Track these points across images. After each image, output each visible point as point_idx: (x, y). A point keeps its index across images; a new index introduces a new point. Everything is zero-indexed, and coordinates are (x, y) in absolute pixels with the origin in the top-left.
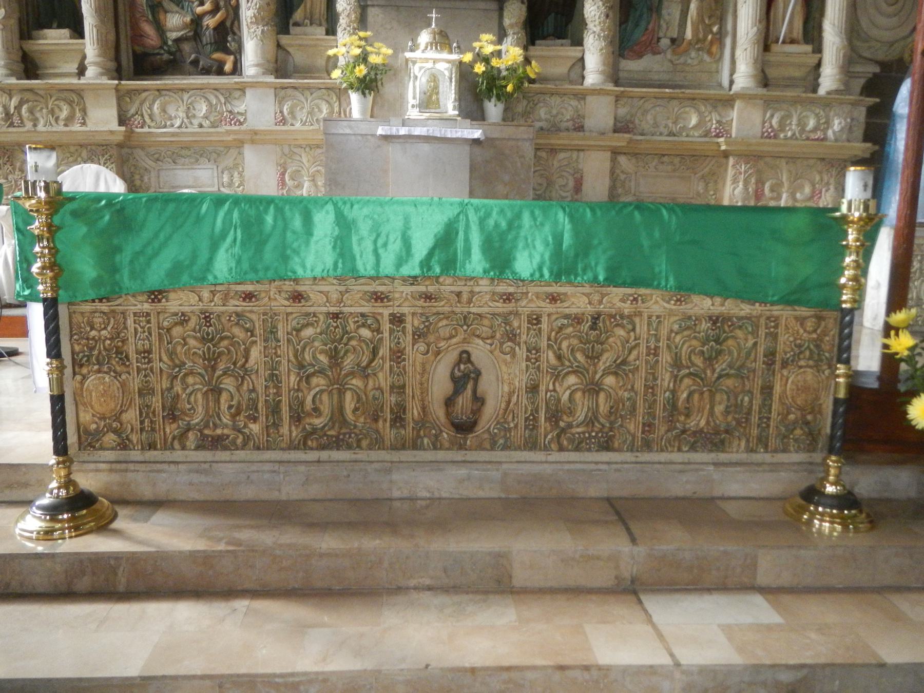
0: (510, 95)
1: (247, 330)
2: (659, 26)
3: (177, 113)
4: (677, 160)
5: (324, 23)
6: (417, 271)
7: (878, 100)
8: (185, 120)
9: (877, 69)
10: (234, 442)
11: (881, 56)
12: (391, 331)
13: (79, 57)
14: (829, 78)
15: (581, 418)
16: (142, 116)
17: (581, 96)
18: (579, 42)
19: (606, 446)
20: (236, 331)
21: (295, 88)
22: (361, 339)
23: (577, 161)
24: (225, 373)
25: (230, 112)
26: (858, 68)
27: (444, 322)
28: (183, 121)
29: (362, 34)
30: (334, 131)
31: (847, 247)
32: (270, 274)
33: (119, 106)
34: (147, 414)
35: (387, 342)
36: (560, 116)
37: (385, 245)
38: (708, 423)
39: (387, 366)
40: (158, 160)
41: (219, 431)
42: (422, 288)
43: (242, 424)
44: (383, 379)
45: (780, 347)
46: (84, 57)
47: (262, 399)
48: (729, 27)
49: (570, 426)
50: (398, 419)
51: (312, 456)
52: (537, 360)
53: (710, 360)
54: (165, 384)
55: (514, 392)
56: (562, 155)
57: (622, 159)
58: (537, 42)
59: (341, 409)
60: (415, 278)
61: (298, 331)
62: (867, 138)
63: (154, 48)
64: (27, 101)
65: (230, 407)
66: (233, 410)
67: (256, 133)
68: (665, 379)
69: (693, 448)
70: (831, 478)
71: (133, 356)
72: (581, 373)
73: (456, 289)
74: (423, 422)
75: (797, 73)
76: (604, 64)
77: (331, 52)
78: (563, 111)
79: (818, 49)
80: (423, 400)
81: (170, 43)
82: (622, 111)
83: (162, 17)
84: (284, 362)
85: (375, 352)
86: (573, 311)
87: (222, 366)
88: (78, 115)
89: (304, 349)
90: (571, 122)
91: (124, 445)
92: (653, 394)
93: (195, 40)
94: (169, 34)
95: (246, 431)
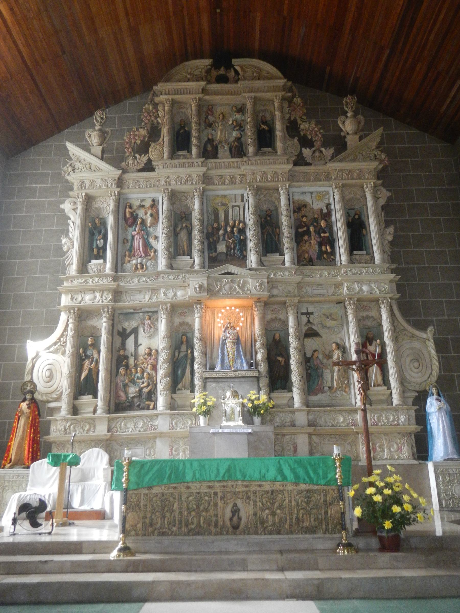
0: (263, 414)
1: (174, 498)
2: (323, 383)
3: (131, 426)
4: (337, 436)
5: (189, 388)
6: (221, 479)
7: (418, 407)
9: (417, 394)
10: (168, 533)
11: (417, 389)
12: (214, 497)
13: (94, 406)
16: (117, 428)
17: (293, 412)
18: (291, 391)
19: (279, 533)
20: (171, 499)
22: (205, 500)
23: (294, 439)
24: (167, 511)
25: (152, 425)
26: (409, 394)
27: (229, 494)
29: (204, 393)
30: (193, 432)
31: (337, 467)
32: (181, 481)
35: (213, 501)
36: (285, 421)
37: (212, 472)
38: (309, 524)
39: (213, 508)
41: (164, 530)
42: (222, 484)
43: (171, 528)
44: (212, 512)
45: (328, 499)
46: (97, 406)
48: (352, 381)
49: (267, 526)
50: (216, 525)
51: (191, 537)
52: (256, 505)
53: (308, 503)
54: (150, 515)
56: (287, 437)
57: (314, 437)
58: (274, 391)
59: (200, 523)
60: (220, 481)
61: (188, 498)
62: (418, 423)
63: (123, 401)
64: (74, 424)
65: (168, 522)
67: (162, 433)
69: (306, 533)
70: (344, 538)
71: (142, 507)
73: (232, 484)
74: (223, 526)
75: (383, 398)
76: (301, 399)
77: (193, 401)
79: (389, 388)
80: (223, 519)
81: (130, 398)
82: (311, 417)
83: (127, 389)
84: (184, 507)
85: (209, 504)
86: (266, 489)
87: (166, 509)
88: (92, 428)
89: (189, 503)
91: (137, 535)
92: (292, 515)
93: (139, 397)
94: (129, 395)
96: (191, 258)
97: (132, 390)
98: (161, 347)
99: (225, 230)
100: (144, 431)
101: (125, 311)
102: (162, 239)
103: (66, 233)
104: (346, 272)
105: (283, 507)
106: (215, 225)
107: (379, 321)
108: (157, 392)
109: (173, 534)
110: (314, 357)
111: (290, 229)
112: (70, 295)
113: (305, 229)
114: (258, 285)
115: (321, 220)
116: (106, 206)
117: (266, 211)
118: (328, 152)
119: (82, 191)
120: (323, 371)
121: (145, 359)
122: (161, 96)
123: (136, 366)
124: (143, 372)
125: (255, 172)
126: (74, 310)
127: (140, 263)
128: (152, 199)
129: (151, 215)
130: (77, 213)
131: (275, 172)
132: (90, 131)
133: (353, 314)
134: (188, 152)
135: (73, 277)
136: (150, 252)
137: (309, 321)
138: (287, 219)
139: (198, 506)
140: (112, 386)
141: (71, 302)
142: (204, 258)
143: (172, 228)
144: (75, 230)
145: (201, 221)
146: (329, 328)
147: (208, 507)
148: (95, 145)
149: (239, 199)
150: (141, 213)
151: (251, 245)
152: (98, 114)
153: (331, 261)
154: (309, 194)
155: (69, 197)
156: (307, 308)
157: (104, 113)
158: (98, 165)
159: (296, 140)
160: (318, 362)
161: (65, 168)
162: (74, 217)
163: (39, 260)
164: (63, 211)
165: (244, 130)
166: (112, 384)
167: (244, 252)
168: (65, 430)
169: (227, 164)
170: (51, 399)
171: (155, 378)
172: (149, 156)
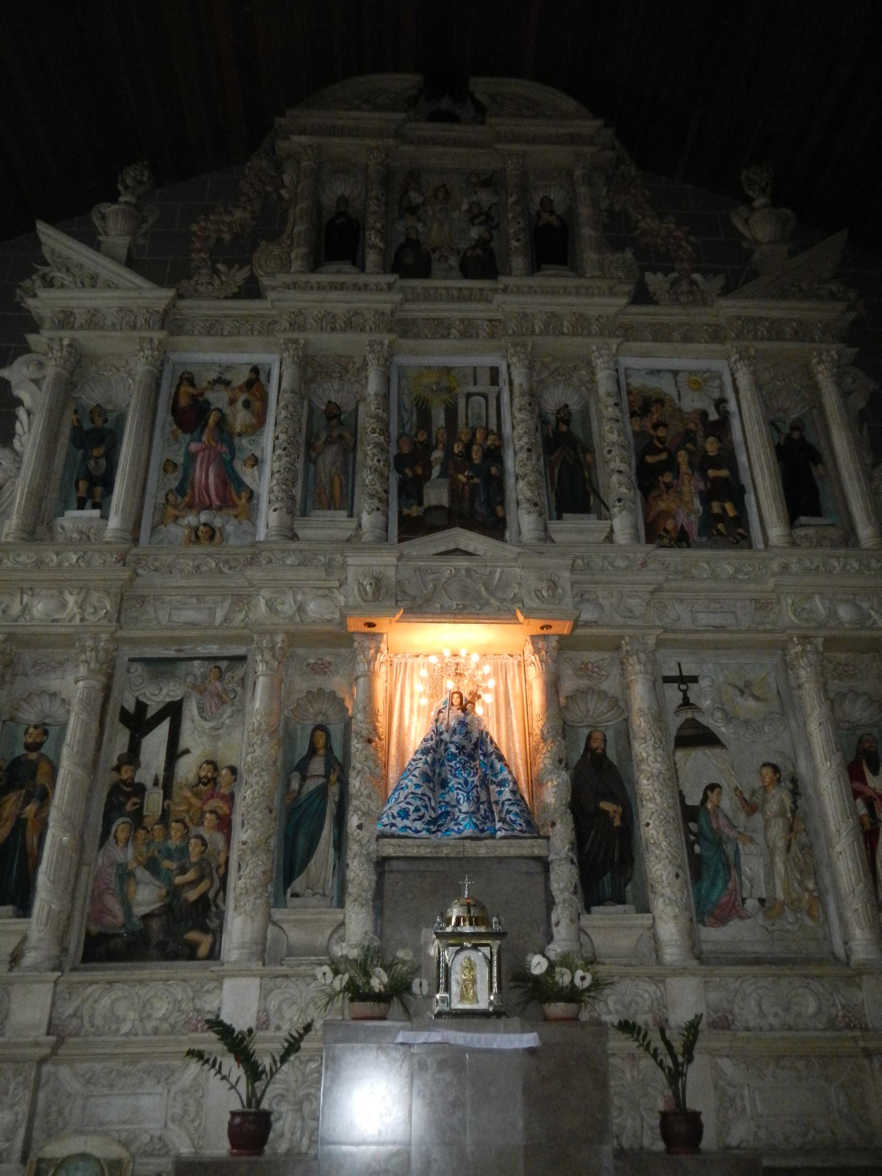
2: (741, 883)
16: (81, 1018)
18: (644, 908)
21: (286, 976)
40: (88, 1082)
46: (25, 939)
58: (594, 909)
78: (639, 999)
82: (713, 996)
83: (131, 890)
96: (351, 515)
99: (448, 450)
102: (271, 462)
104: (785, 567)
106: (422, 437)
108: (224, 900)
110: (709, 806)
113: (664, 456)
115: (706, 437)
119: (62, 334)
120: (737, 852)
121: (197, 795)
122: (295, 138)
123: (165, 818)
124: (186, 837)
125: (528, 311)
127: (205, 524)
128: (250, 367)
131: (582, 315)
133: (817, 681)
137: (686, 703)
140: (83, 877)
143: (302, 439)
144: (29, 430)
146: (747, 723)
149: (485, 378)
152: (130, 175)
153: (738, 542)
154: (670, 375)
155: (27, 350)
159: (629, 254)
160: (722, 821)
162: (33, 396)
165: (498, 225)
166: (85, 870)
167: (499, 509)
169: (455, 292)
172: (252, 269)
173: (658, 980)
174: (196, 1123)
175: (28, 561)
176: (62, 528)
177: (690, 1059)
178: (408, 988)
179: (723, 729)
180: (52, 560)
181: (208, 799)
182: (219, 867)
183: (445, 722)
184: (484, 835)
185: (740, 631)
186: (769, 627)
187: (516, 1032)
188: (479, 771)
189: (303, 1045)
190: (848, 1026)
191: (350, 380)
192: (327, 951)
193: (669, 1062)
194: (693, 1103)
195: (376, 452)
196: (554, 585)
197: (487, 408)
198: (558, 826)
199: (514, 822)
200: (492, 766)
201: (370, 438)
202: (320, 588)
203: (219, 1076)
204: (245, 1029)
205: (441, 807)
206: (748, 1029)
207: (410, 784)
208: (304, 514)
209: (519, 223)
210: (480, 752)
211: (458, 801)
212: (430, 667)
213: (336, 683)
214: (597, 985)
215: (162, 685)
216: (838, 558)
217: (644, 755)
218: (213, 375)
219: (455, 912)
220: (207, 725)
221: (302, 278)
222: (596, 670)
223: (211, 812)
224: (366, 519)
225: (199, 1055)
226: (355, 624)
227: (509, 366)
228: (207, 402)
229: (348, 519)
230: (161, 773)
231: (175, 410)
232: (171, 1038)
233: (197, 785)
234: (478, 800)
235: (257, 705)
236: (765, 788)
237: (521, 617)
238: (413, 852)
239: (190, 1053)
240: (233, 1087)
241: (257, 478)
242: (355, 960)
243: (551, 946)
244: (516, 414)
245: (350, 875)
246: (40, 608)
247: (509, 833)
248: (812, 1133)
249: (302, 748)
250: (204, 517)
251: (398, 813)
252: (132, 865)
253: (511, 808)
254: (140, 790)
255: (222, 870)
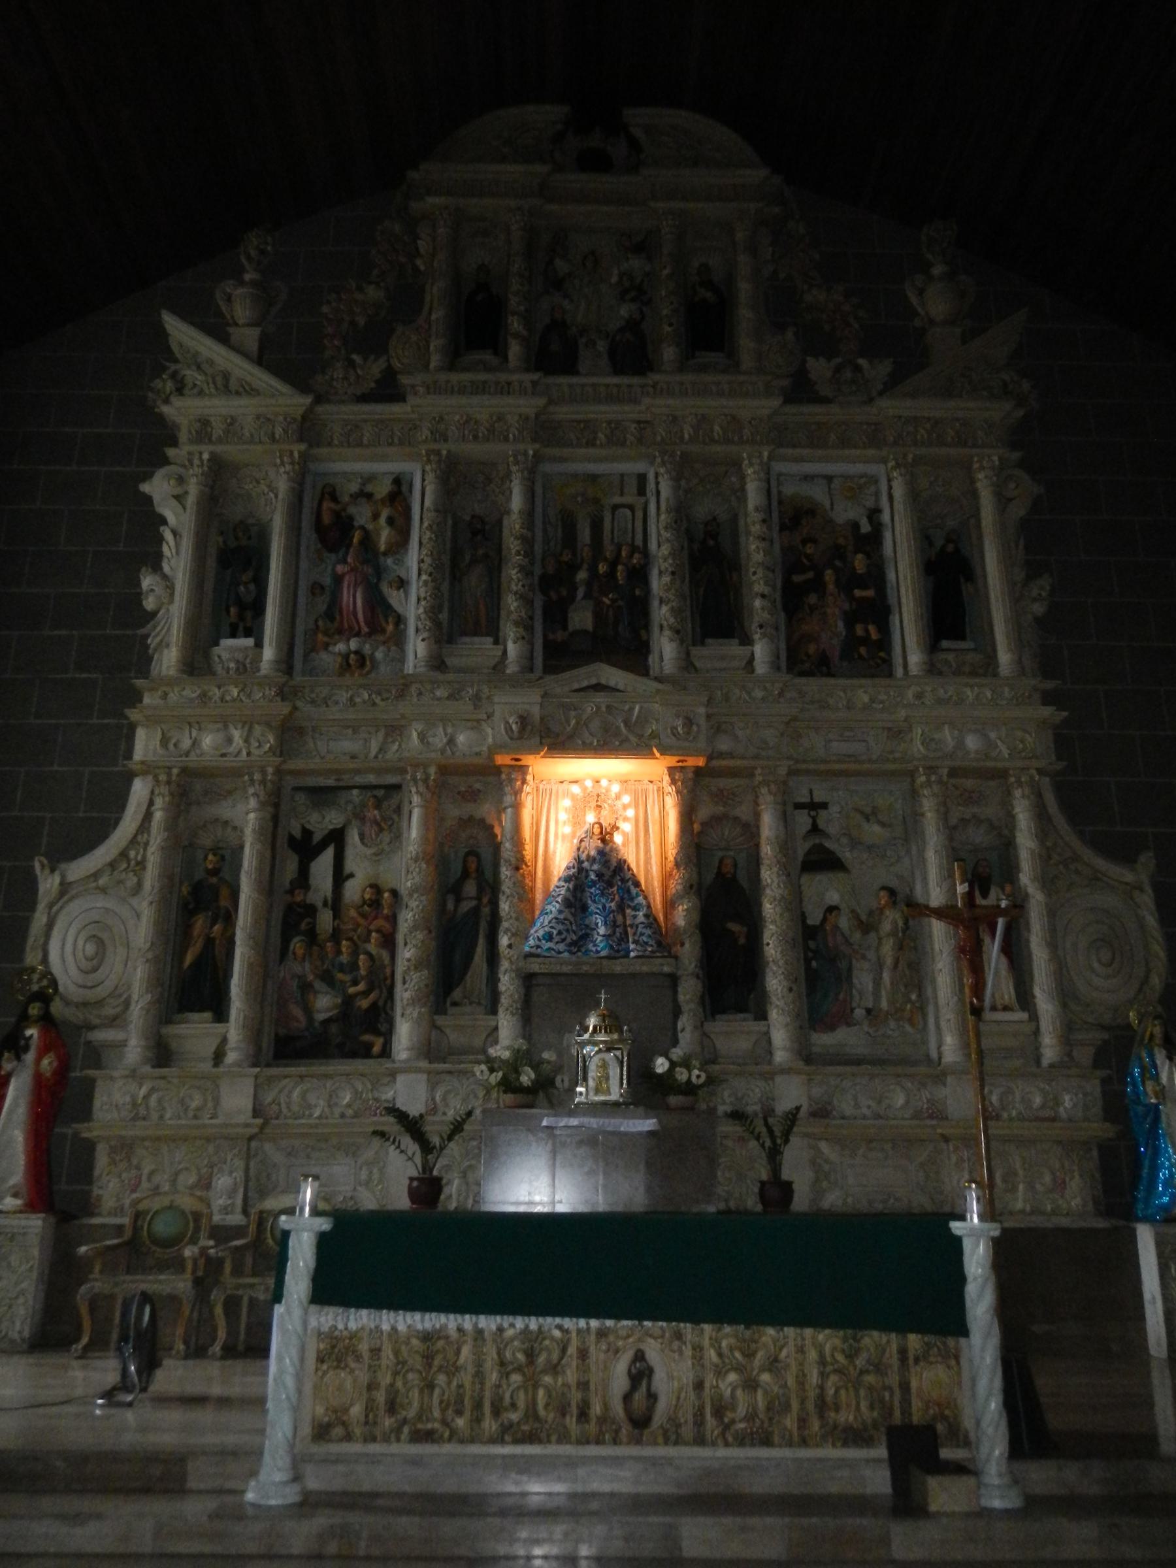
8: (326, 1109)
9: (1106, 1036)
10: (442, 1437)
13: (217, 1041)
14: (1050, 1049)
15: (743, 1414)
16: (279, 1104)
18: (762, 1016)
19: (767, 1442)
21: (450, 1072)
22: (553, 1339)
24: (440, 1369)
28: (323, 1111)
33: (255, 1096)
34: (372, 1409)
38: (855, 1418)
39: (574, 1363)
41: (429, 1426)
43: (449, 1419)
44: (571, 1376)
46: (224, 1040)
47: (468, 1393)
49: (733, 1422)
50: (583, 1415)
52: (701, 1358)
53: (851, 1356)
54: (388, 1379)
55: (682, 1388)
58: (718, 1017)
65: (441, 1402)
66: (443, 1405)
68: (814, 1378)
69: (845, 1444)
72: (742, 1371)
78: (751, 1095)
79: (1034, 1017)
80: (604, 1397)
81: (317, 1024)
82: (817, 1091)
83: (311, 997)
84: (489, 1359)
85: (564, 1350)
87: (436, 1362)
89: (506, 1346)
90: (760, 1105)
95: (453, 1425)
96: (496, 642)
97: (325, 1003)
98: (409, 884)
99: (593, 569)
100: (356, 1116)
101: (311, 781)
102: (416, 588)
103: (155, 561)
104: (919, 696)
105: (779, 1365)
106: (566, 557)
107: (1006, 832)
108: (392, 1009)
109: (454, 1436)
111: (771, 575)
112: (159, 735)
113: (810, 575)
114: (679, 723)
115: (856, 553)
116: (266, 490)
117: (706, 524)
118: (877, 371)
119: (203, 448)
120: (850, 969)
121: (363, 916)
123: (336, 936)
124: (355, 953)
126: (169, 775)
127: (356, 652)
128: (391, 478)
129: (390, 521)
130: (184, 508)
131: (734, 417)
132: (228, 286)
133: (938, 811)
134: (496, 353)
135: (171, 682)
136: (384, 625)
137: (815, 829)
138: (762, 545)
139: (531, 1355)
141: (161, 751)
142: (531, 644)
143: (446, 559)
144: (178, 553)
145: (527, 542)
146: (870, 848)
147: (561, 1358)
148: (240, 322)
149: (632, 486)
150: (362, 514)
151: (661, 613)
155: (166, 461)
156: (811, 792)
157: (269, 239)
158: (249, 378)
160: (839, 938)
161: (158, 384)
163: (74, 632)
164: (149, 500)
167: (643, 633)
168: (134, 1104)
170: (97, 1021)
171: (388, 971)
172: (388, 361)
173: (769, 1077)
174: (380, 1187)
175: (194, 695)
176: (219, 657)
177: (787, 1141)
178: (552, 1083)
179: (848, 854)
180: (215, 694)
181: (374, 920)
182: (386, 979)
183: (586, 852)
184: (617, 955)
185: (870, 761)
186: (897, 755)
187: (640, 1118)
188: (617, 897)
189: (466, 1127)
190: (931, 1117)
191: (494, 491)
192: (484, 1052)
193: (768, 1143)
194: (786, 1175)
195: (521, 577)
196: (689, 722)
197: (633, 520)
198: (687, 946)
199: (646, 943)
200: (629, 891)
201: (515, 561)
202: (469, 720)
203: (398, 1151)
204: (417, 1114)
205: (581, 930)
206: (843, 1118)
207: (553, 909)
208: (451, 640)
209: (672, 303)
210: (618, 878)
211: (597, 924)
212: (574, 798)
213: (485, 810)
214: (710, 1081)
215: (324, 812)
216: (972, 687)
217: (769, 881)
218: (354, 487)
219: (592, 1022)
220: (369, 851)
221: (442, 377)
222: (731, 797)
223: (378, 931)
224: (512, 648)
225: (382, 1135)
226: (502, 759)
227: (657, 475)
228: (351, 518)
229: (495, 646)
230: (329, 894)
231: (319, 526)
232: (355, 1120)
233: (362, 906)
234: (614, 925)
235: (414, 833)
236: (881, 910)
237: (658, 755)
238: (556, 969)
239: (375, 1133)
240: (410, 1159)
241: (404, 602)
242: (508, 1061)
243: (674, 1050)
244: (662, 532)
245: (502, 987)
246: (208, 741)
247: (640, 954)
248: (892, 1201)
249: (456, 868)
250: (354, 644)
251: (543, 936)
252: (311, 977)
253: (644, 931)
254: (311, 910)
255: (388, 982)
